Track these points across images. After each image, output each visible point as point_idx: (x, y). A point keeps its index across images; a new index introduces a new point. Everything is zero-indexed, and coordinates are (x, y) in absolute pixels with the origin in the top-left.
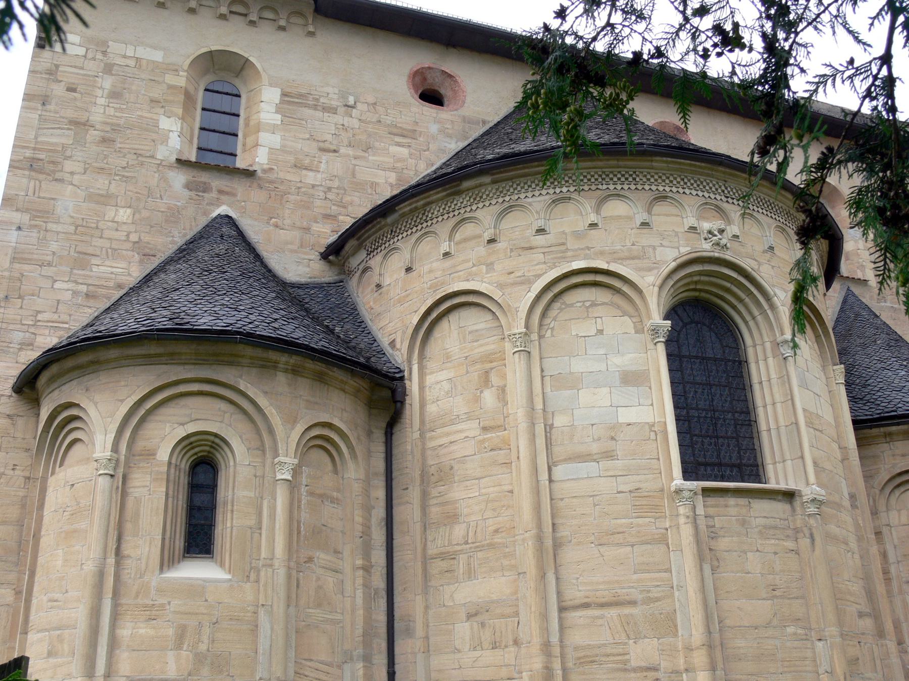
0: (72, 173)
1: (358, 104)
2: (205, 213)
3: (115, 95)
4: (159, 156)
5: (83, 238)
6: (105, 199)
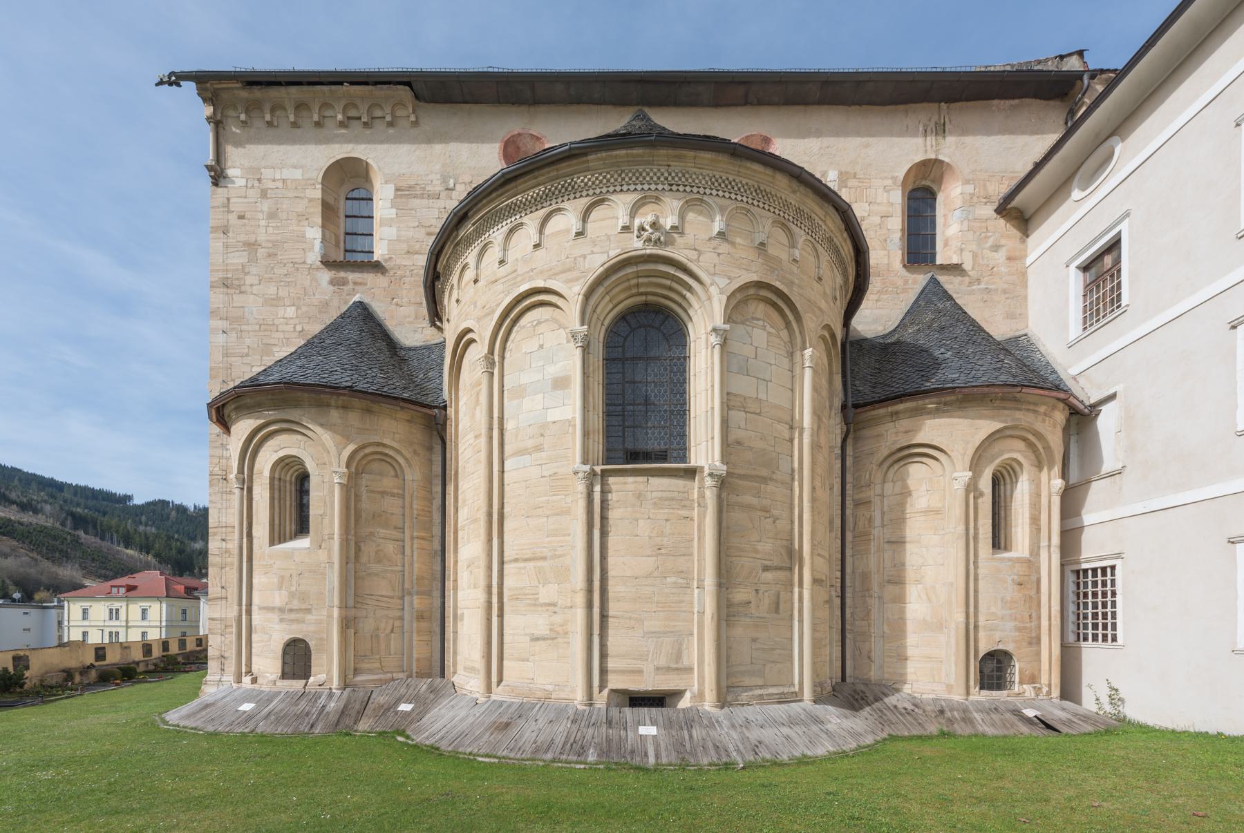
0: (252, 285)
1: (457, 185)
2: (346, 303)
3: (272, 215)
4: (309, 262)
5: (266, 333)
6: (276, 301)
